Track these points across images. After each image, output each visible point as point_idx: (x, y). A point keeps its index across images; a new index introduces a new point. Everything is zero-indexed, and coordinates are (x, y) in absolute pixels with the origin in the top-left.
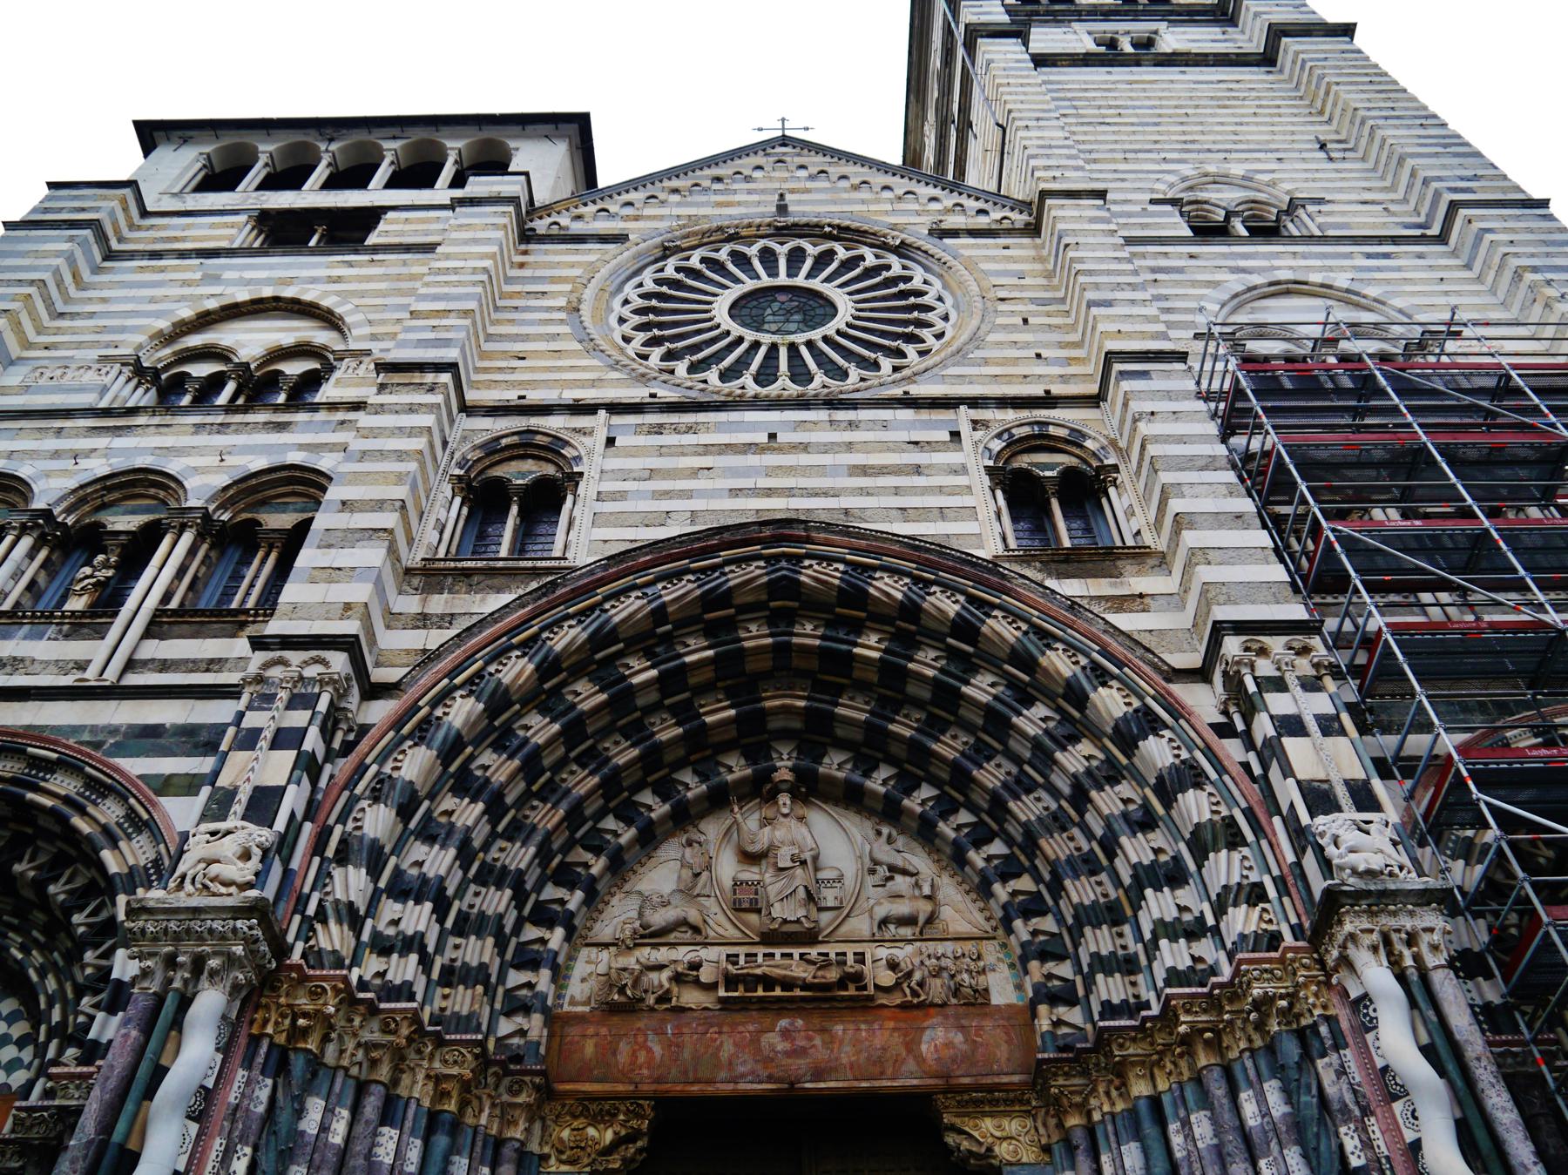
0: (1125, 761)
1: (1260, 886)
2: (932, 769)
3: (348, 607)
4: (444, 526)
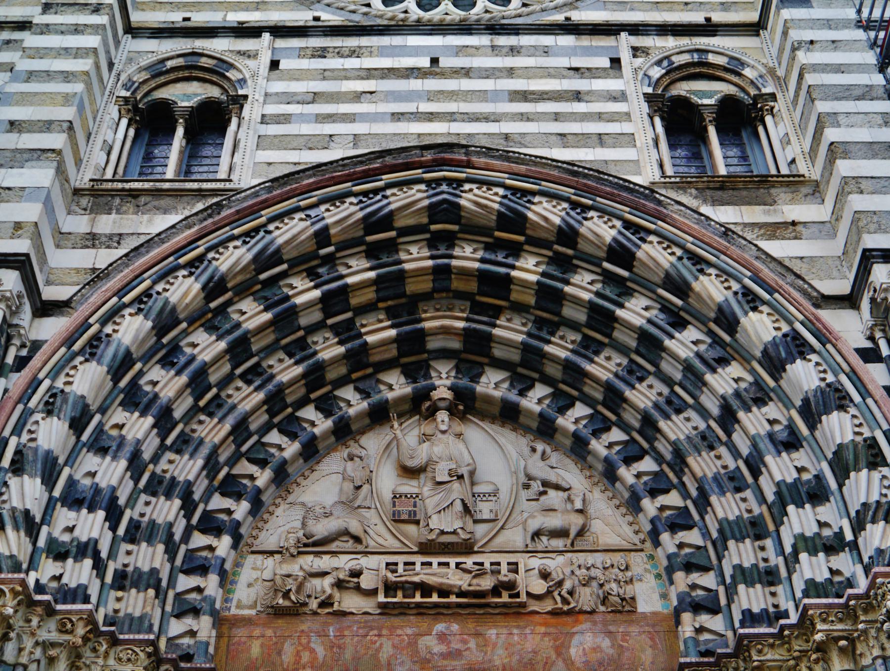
0: (771, 383)
2: (586, 389)
3: (18, 226)
4: (111, 148)
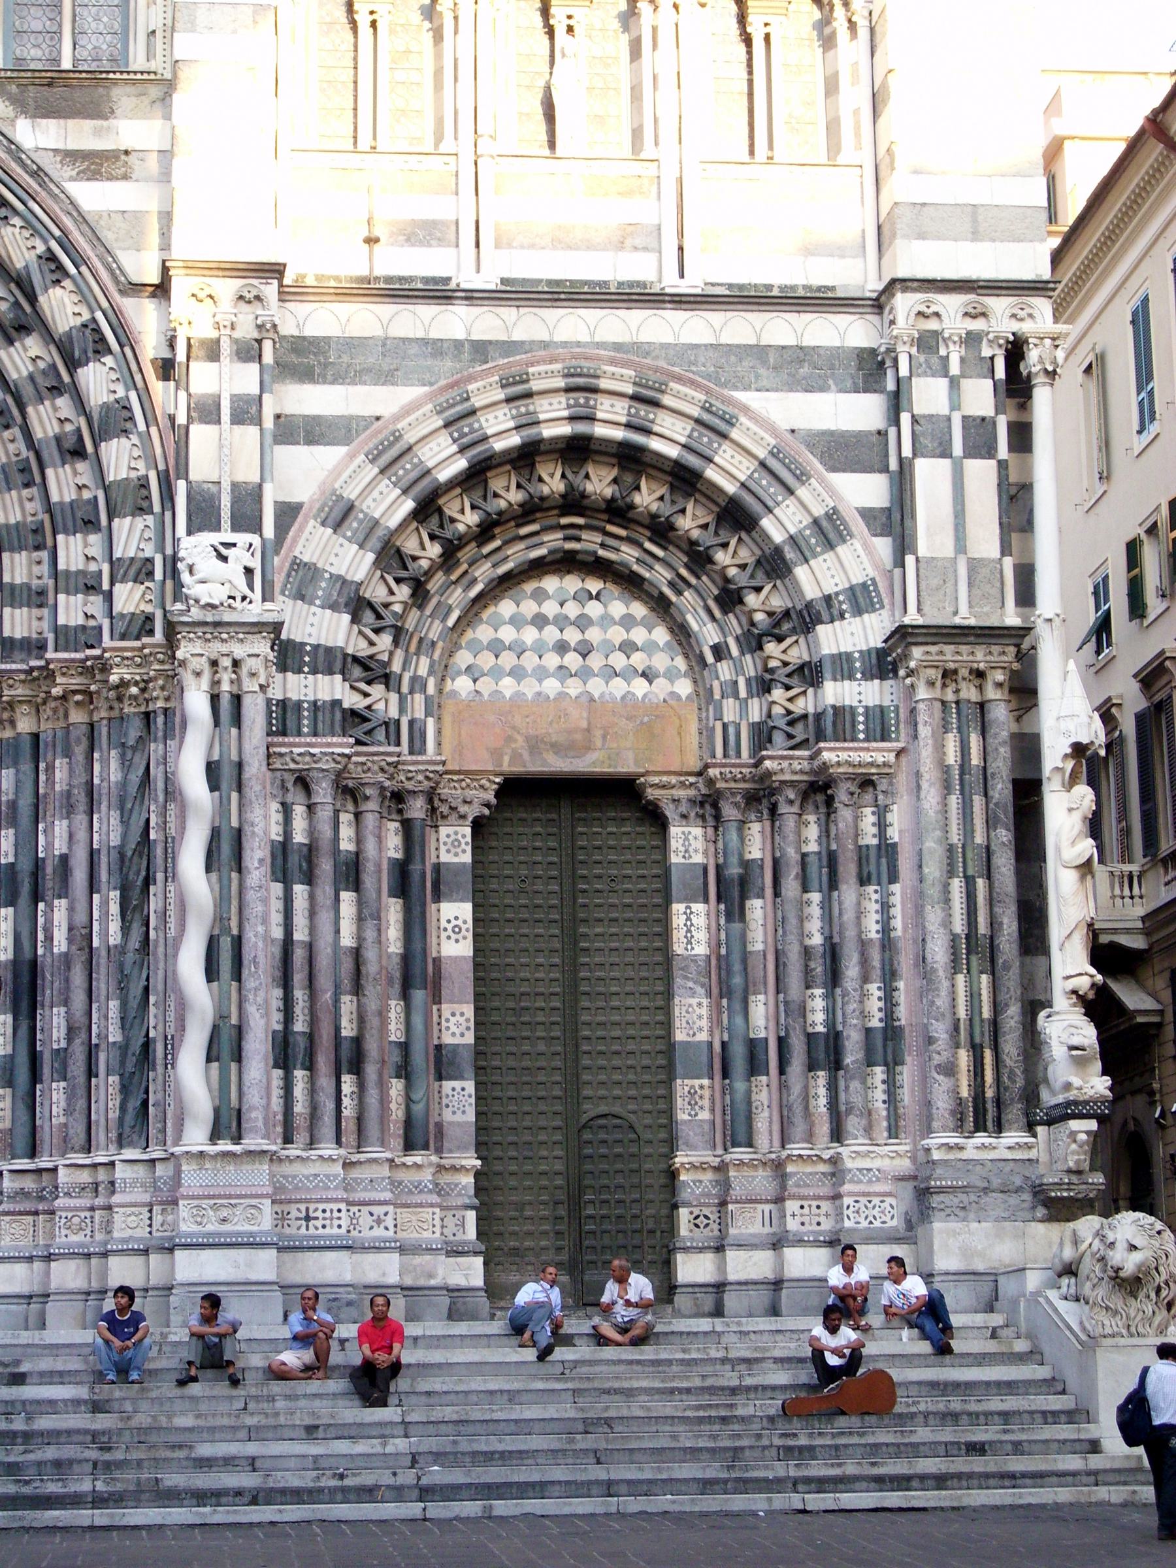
1: (150, 561)
